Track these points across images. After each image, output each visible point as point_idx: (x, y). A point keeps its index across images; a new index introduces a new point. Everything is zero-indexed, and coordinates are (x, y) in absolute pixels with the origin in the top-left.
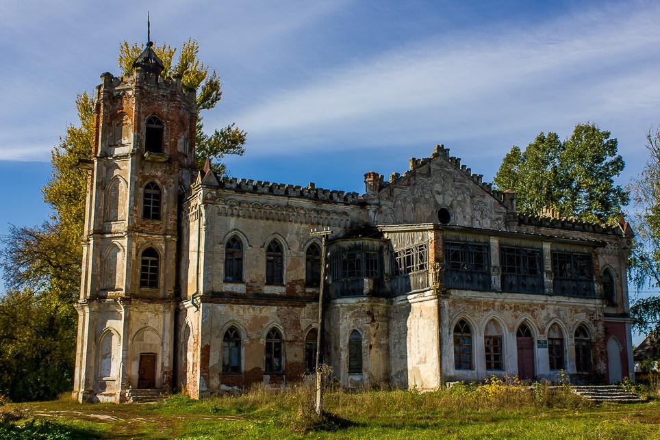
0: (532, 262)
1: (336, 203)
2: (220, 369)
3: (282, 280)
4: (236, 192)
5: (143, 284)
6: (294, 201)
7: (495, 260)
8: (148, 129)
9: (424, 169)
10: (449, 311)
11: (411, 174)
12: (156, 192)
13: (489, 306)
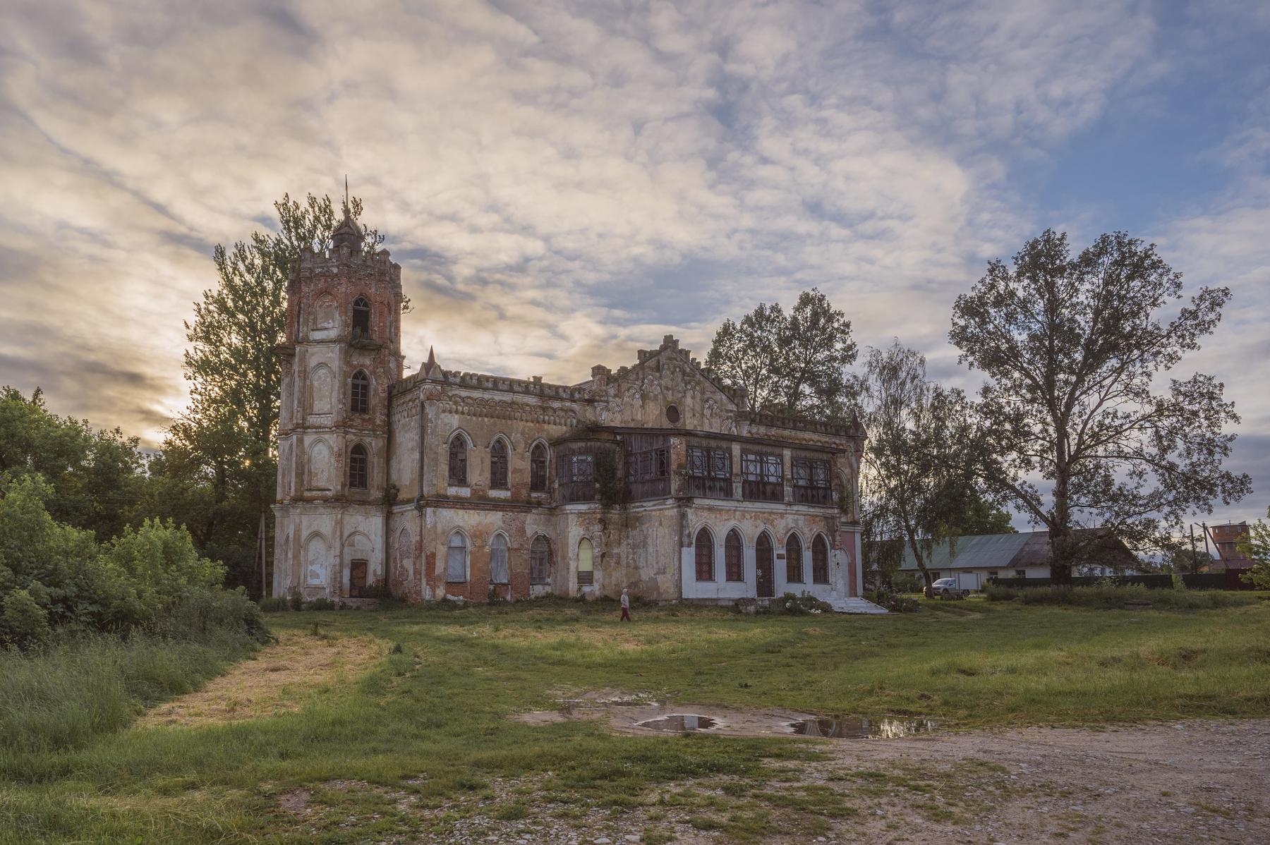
3: (506, 483)
5: (352, 485)
6: (520, 398)
8: (355, 310)
9: (652, 363)
11: (641, 366)
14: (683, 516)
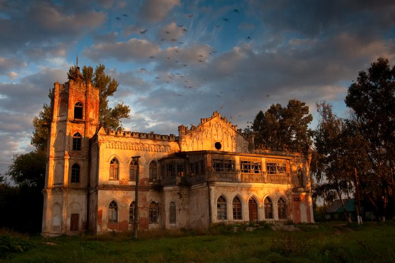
0: (256, 167)
1: (164, 141)
2: (107, 221)
4: (115, 136)
7: (238, 167)
8: (75, 108)
10: (215, 192)
12: (79, 137)
13: (235, 188)
14: (209, 190)
